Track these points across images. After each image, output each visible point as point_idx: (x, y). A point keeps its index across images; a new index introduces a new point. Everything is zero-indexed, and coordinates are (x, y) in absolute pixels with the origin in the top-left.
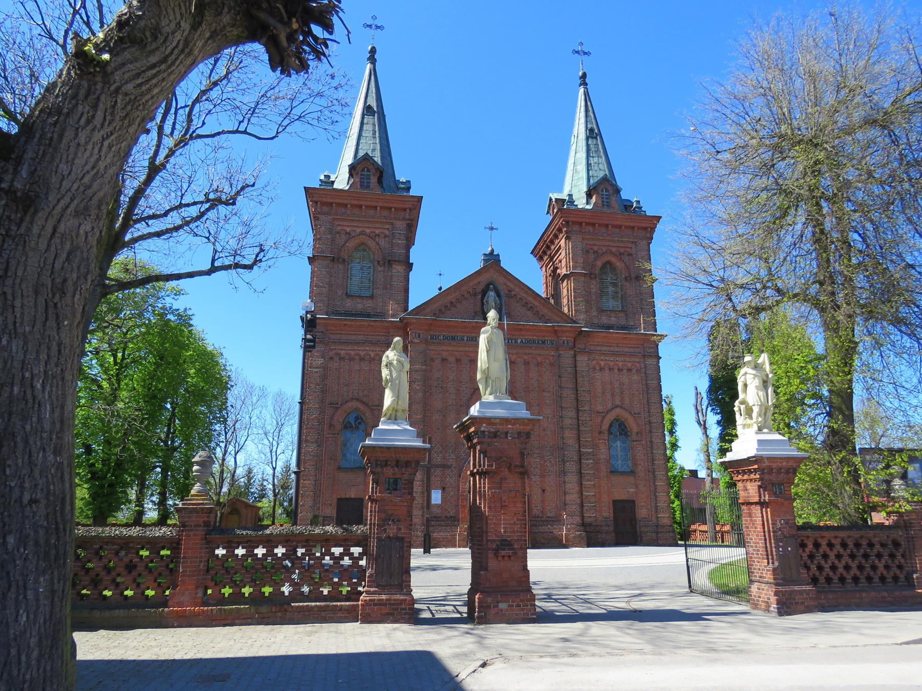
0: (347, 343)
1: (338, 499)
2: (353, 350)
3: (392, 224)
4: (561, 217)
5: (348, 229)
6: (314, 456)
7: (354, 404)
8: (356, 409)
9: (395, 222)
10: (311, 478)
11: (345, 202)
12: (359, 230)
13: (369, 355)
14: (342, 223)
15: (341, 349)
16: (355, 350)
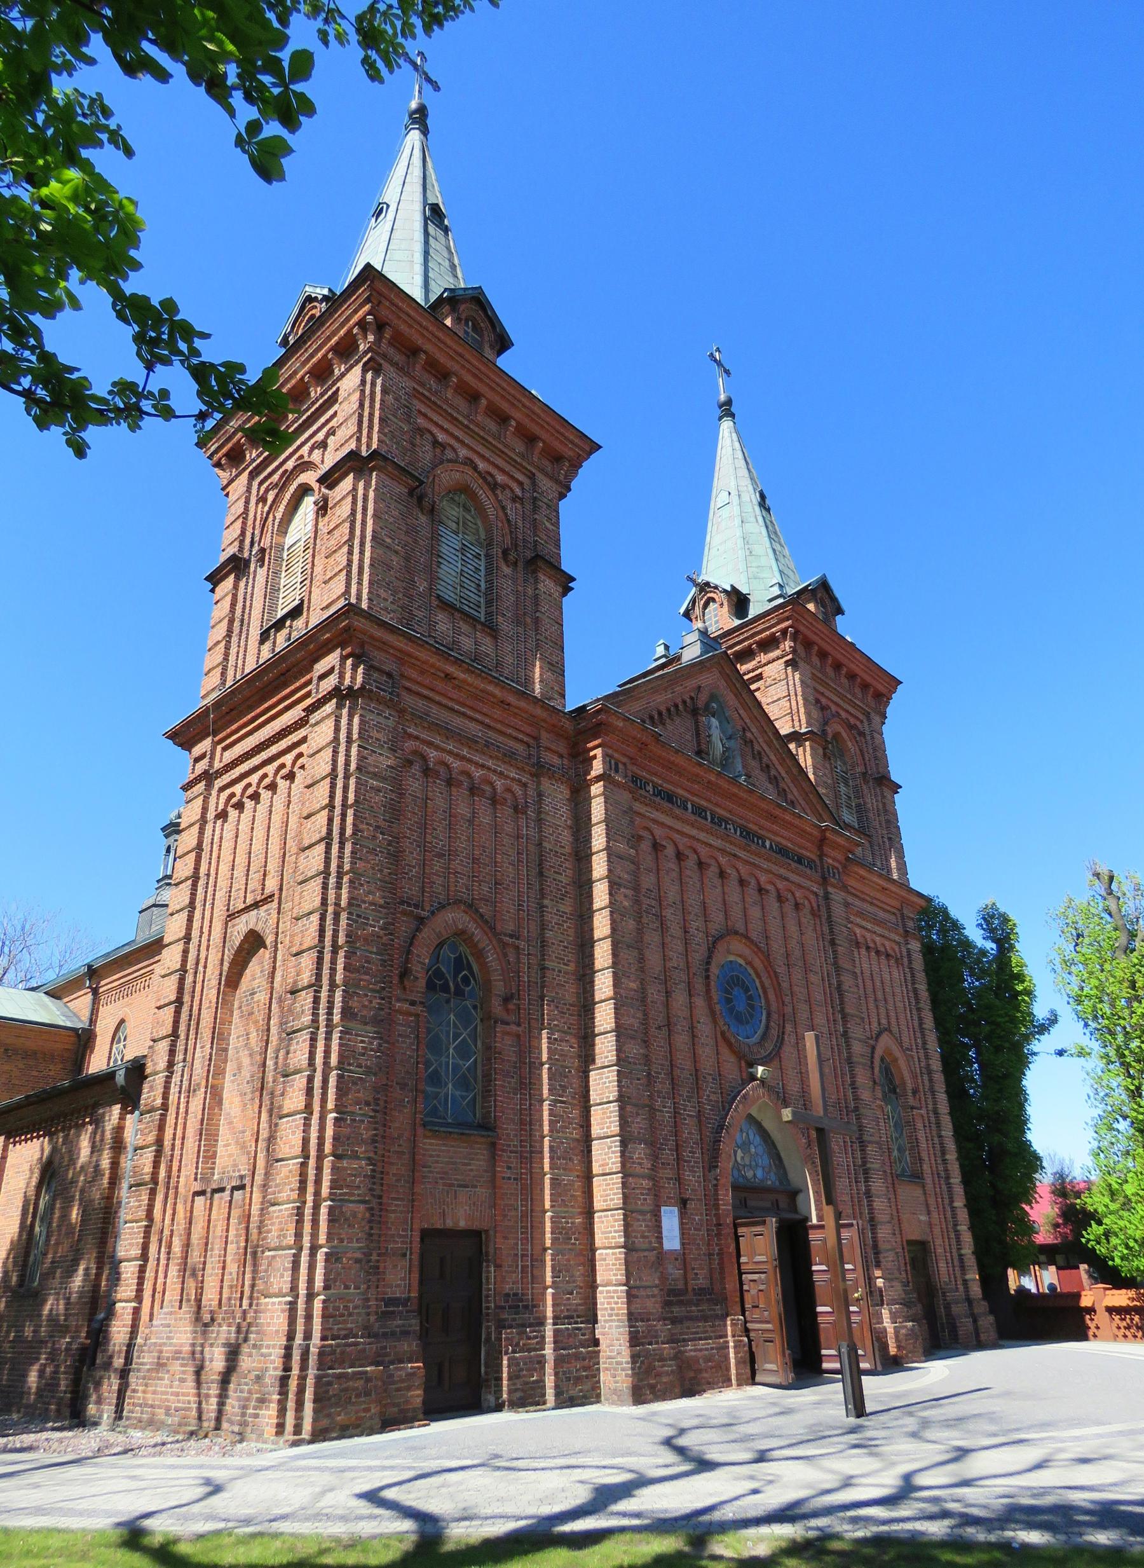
0: (448, 733)
1: (426, 1234)
2: (457, 756)
3: (532, 477)
4: (787, 619)
5: (441, 437)
6: (368, 1071)
7: (454, 918)
8: (463, 932)
9: (539, 476)
10: (360, 1150)
11: (449, 364)
12: (463, 452)
13: (491, 784)
14: (430, 414)
15: (430, 744)
16: (463, 758)
